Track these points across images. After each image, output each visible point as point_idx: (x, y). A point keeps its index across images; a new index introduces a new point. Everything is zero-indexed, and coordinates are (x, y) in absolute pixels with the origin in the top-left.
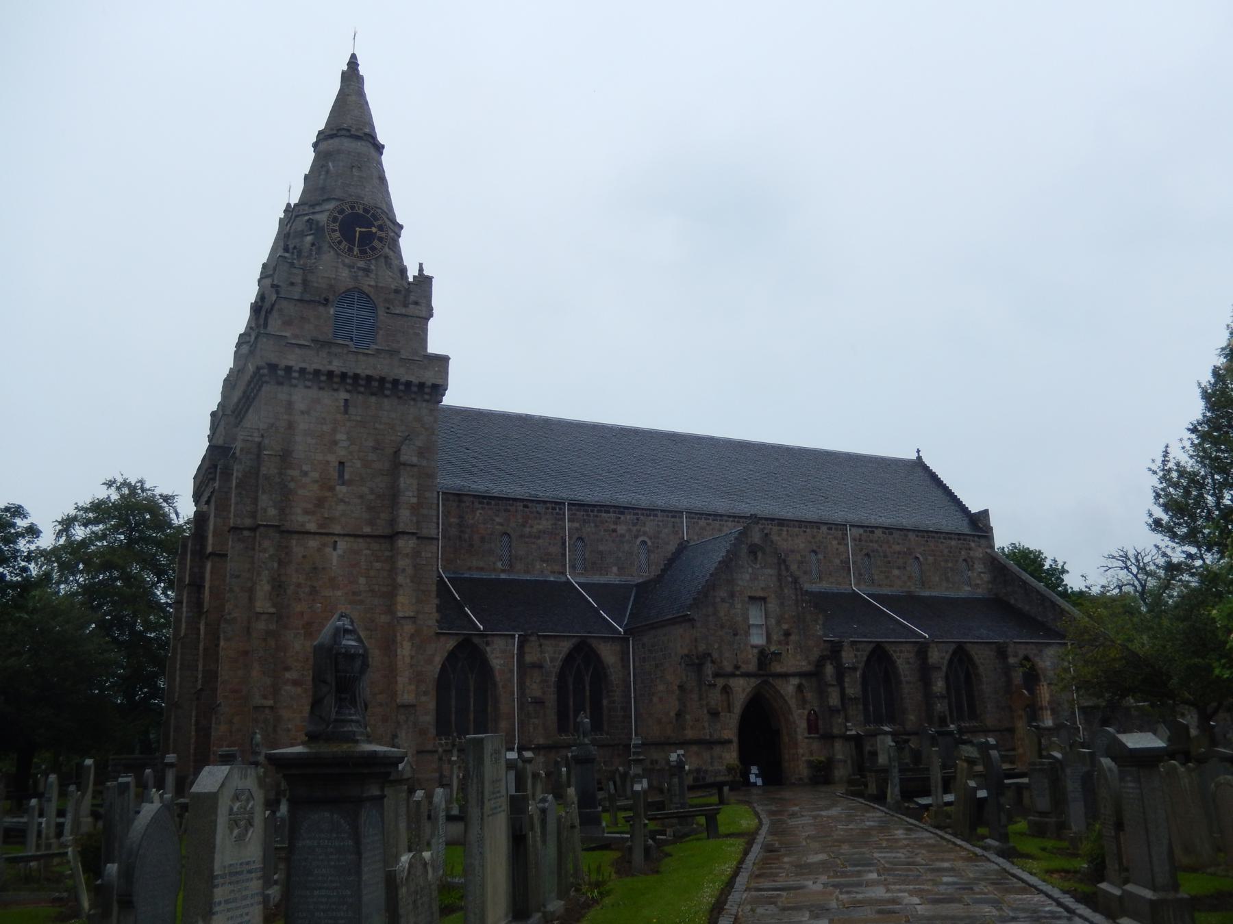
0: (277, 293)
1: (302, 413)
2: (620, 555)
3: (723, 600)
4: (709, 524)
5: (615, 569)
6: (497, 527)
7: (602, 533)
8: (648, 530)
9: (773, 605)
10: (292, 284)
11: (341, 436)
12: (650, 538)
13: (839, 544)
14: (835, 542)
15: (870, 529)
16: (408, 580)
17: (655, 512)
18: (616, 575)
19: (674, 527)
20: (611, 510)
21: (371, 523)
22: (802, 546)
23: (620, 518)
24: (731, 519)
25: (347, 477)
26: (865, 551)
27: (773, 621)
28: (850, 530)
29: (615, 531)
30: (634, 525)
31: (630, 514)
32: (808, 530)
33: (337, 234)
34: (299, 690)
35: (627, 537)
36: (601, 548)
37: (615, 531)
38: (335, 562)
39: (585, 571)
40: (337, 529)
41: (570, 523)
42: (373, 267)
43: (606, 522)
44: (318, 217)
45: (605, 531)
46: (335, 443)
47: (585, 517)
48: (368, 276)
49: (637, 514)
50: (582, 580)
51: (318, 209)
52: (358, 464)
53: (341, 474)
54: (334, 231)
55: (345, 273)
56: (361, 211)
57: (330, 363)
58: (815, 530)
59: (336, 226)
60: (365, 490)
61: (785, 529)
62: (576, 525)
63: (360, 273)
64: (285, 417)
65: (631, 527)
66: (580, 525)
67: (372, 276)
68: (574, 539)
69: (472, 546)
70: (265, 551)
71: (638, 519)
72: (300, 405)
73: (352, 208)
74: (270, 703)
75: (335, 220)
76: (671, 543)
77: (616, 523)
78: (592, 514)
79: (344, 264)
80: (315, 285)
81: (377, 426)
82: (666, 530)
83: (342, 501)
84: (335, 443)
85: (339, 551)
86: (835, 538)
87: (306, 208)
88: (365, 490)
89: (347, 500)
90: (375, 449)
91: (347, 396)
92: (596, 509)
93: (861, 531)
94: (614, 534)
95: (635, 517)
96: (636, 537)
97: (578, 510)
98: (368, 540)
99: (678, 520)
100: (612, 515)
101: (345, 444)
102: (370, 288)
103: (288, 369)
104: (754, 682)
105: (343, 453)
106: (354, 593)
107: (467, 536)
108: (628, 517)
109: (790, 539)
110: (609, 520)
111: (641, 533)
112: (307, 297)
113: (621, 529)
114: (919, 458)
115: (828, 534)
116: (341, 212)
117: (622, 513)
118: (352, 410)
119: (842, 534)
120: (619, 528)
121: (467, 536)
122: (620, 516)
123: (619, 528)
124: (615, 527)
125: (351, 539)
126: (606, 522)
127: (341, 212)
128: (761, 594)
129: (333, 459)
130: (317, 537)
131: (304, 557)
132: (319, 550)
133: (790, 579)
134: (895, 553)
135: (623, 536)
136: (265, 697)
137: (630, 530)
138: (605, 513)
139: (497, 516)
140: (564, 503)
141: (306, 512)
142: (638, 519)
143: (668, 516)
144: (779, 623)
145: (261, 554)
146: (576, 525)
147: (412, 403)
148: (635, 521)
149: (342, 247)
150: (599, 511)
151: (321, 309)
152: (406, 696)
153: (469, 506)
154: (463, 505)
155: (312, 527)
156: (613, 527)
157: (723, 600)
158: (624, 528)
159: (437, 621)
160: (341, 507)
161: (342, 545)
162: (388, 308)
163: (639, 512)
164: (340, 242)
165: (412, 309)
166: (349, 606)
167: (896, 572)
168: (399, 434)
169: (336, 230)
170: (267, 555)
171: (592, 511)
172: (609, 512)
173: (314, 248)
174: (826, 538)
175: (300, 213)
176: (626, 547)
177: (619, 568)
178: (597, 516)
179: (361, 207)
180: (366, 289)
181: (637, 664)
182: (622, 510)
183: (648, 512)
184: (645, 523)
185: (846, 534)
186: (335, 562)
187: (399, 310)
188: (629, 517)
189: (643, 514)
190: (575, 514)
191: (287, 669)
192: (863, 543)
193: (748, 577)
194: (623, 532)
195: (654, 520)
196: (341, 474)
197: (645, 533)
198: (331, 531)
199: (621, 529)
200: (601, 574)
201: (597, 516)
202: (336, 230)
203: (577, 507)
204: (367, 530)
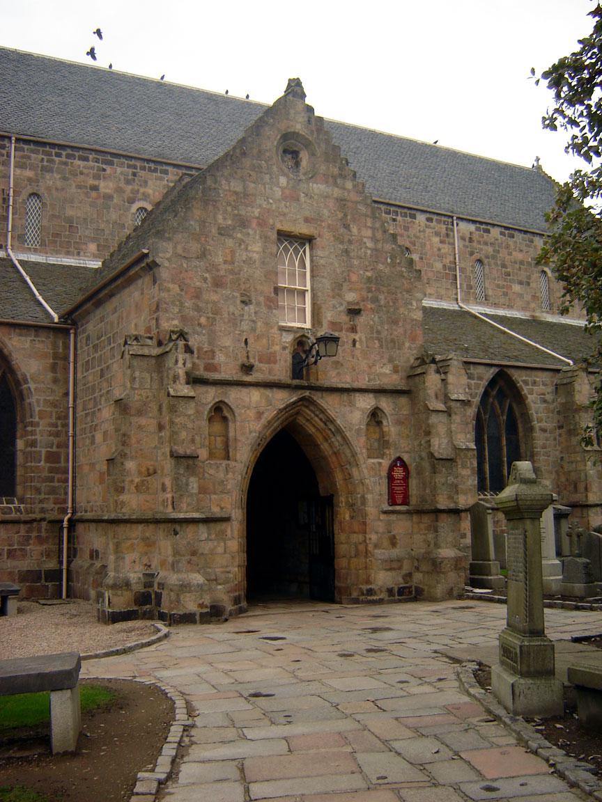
2: (102, 226)
3: (223, 232)
7: (73, 190)
8: (151, 192)
9: (327, 250)
13: (442, 242)
14: (436, 240)
15: (485, 226)
17: (165, 167)
20: (91, 156)
23: (104, 170)
26: (477, 256)
27: (326, 284)
28: (457, 225)
29: (95, 188)
30: (128, 182)
31: (122, 165)
32: (399, 218)
35: (115, 201)
36: (70, 212)
37: (95, 188)
39: (41, 245)
41: (18, 171)
43: (82, 173)
45: (79, 187)
47: (45, 163)
49: (135, 167)
58: (408, 219)
62: (29, 173)
65: (122, 185)
66: (36, 175)
68: (24, 195)
77: (97, 177)
78: (57, 159)
86: (437, 234)
92: (64, 153)
93: (472, 227)
94: (94, 194)
95: (131, 171)
96: (131, 201)
97: (33, 151)
100: (91, 163)
108: (119, 170)
110: (85, 171)
111: (140, 196)
113: (106, 187)
114: (539, 168)
115: (427, 227)
117: (111, 163)
119: (447, 229)
120: (102, 184)
122: (104, 167)
123: (102, 184)
124: (96, 183)
126: (82, 173)
128: (303, 229)
133: (362, 209)
134: (515, 263)
135: (109, 197)
137: (120, 190)
138: (79, 160)
140: (10, 138)
142: (134, 174)
144: (338, 288)
146: (29, 173)
148: (130, 177)
150: (68, 156)
156: (91, 182)
157: (223, 232)
163: (138, 164)
167: (517, 288)
171: (59, 155)
172: (86, 159)
174: (424, 231)
177: (98, 246)
182: (109, 158)
183: (152, 166)
184: (146, 182)
185: (452, 230)
188: (119, 170)
189: (143, 168)
190: (29, 158)
192: (475, 244)
193: (278, 193)
194: (107, 191)
195: (161, 179)
197: (146, 197)
201: (66, 164)
203: (32, 147)
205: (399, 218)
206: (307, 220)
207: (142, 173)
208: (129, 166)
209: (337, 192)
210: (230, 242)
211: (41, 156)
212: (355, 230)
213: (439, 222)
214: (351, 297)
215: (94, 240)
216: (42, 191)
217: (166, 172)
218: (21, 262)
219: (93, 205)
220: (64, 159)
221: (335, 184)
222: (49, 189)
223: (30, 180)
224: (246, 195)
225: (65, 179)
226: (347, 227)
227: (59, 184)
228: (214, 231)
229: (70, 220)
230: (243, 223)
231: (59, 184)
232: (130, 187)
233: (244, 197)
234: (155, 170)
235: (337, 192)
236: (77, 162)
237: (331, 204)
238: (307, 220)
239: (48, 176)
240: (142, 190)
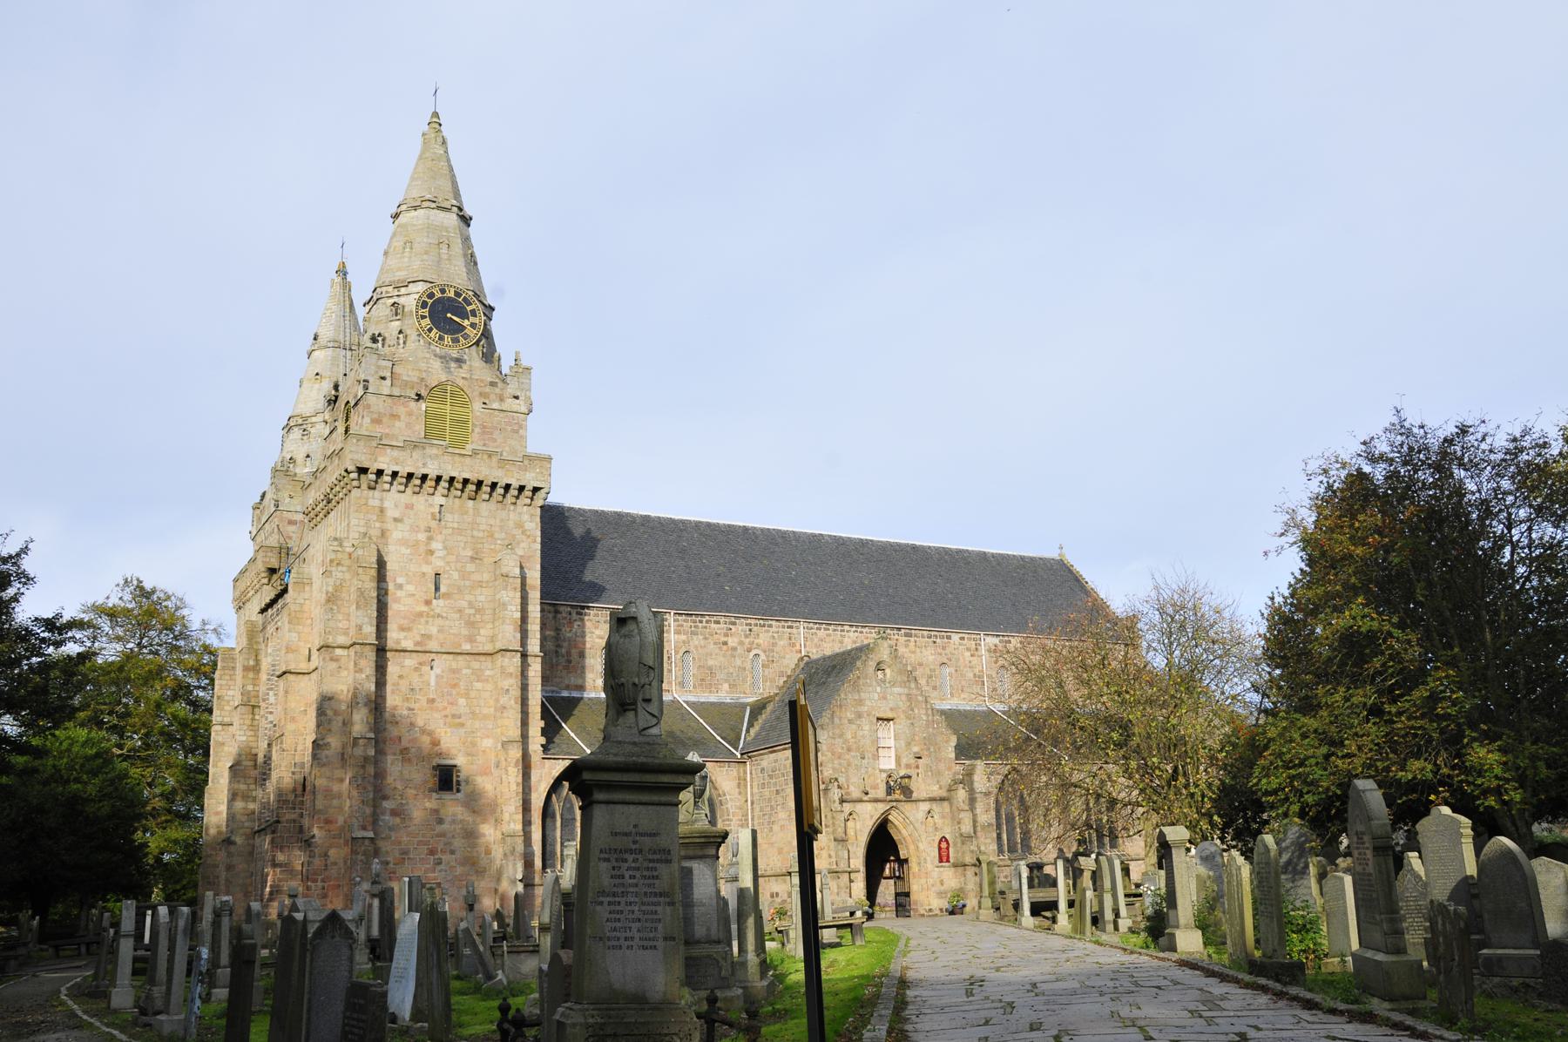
0: (366, 388)
1: (395, 520)
2: (731, 671)
3: (850, 721)
4: (829, 635)
5: (726, 686)
6: (597, 640)
9: (902, 724)
10: (383, 378)
11: (435, 545)
12: (765, 652)
14: (968, 654)
16: (513, 702)
18: (727, 692)
19: (790, 639)
20: (722, 620)
21: (471, 639)
22: (931, 658)
24: (854, 629)
25: (443, 589)
27: (903, 743)
29: (725, 643)
30: (746, 636)
31: (742, 624)
32: (938, 640)
33: (427, 321)
34: (398, 820)
36: (710, 663)
37: (725, 643)
38: (433, 683)
40: (433, 645)
42: (466, 357)
44: (402, 300)
45: (715, 644)
46: (431, 552)
48: (461, 367)
50: (692, 699)
51: (403, 291)
52: (456, 575)
53: (437, 589)
54: (423, 317)
55: (437, 364)
56: (452, 295)
57: (424, 465)
59: (426, 312)
60: (464, 604)
61: (912, 639)
63: (453, 365)
64: (378, 525)
65: (743, 639)
67: (465, 367)
69: (570, 662)
70: (361, 671)
71: (750, 630)
72: (391, 513)
73: (443, 291)
74: (371, 834)
75: (424, 305)
76: (787, 656)
77: (726, 635)
79: (436, 355)
80: (405, 378)
81: (475, 533)
82: (782, 643)
83: (439, 616)
84: (431, 552)
85: (437, 670)
86: (968, 649)
87: (390, 289)
88: (464, 604)
89: (444, 615)
90: (473, 559)
91: (443, 501)
94: (725, 647)
95: (748, 627)
96: (749, 651)
98: (467, 657)
99: (794, 631)
101: (441, 554)
102: (466, 382)
103: (380, 473)
104: (882, 807)
105: (440, 563)
106: (454, 716)
107: (564, 651)
108: (740, 628)
109: (918, 650)
111: (755, 646)
112: (396, 392)
116: (431, 295)
117: (734, 624)
118: (448, 517)
121: (564, 651)
124: (725, 639)
125: (451, 657)
127: (431, 295)
128: (890, 715)
129: (429, 571)
130: (414, 654)
131: (400, 677)
132: (416, 669)
133: (920, 698)
135: (734, 649)
136: (364, 828)
137: (741, 643)
139: (596, 628)
141: (402, 629)
142: (750, 630)
143: (783, 627)
144: (908, 744)
145: (357, 675)
146: (683, 637)
147: (512, 507)
149: (432, 335)
150: (707, 622)
151: (413, 404)
152: (512, 826)
153: (565, 618)
154: (559, 616)
155: (408, 644)
157: (850, 721)
158: (736, 640)
159: (542, 746)
160: (439, 621)
161: (441, 663)
162: (484, 403)
164: (430, 330)
165: (510, 404)
166: (448, 730)
168: (499, 542)
169: (425, 317)
170: (364, 676)
171: (701, 622)
172: (718, 623)
173: (401, 336)
175: (383, 295)
176: (738, 662)
178: (706, 627)
179: (452, 290)
180: (461, 383)
181: (755, 790)
185: (980, 645)
186: (433, 683)
187: (495, 405)
190: (682, 626)
191: (385, 798)
194: (734, 645)
195: (768, 631)
196: (437, 589)
197: (758, 645)
198: (427, 648)
199: (732, 642)
200: (710, 692)
201: (706, 627)
202: (425, 317)
204: (467, 647)
205: (938, 640)
206: (891, 709)
207: (755, 629)
208: (747, 625)
209: (906, 691)
210: (854, 727)
211: (690, 624)
212: (916, 711)
213: (969, 639)
214: (916, 749)
215: (726, 681)
216: (692, 649)
217: (770, 626)
218: (686, 702)
219: (724, 656)
220: (704, 624)
221: (905, 687)
222: (696, 647)
223: (684, 642)
224: (861, 701)
225: (705, 638)
226: (912, 710)
227: (702, 643)
228: (846, 722)
229: (710, 668)
230: (859, 716)
231: (702, 643)
232: (748, 640)
233: (860, 702)
234: (764, 626)
235: (906, 691)
236: (713, 625)
237: (904, 698)
238: (891, 709)
239: (695, 637)
240: (756, 641)
